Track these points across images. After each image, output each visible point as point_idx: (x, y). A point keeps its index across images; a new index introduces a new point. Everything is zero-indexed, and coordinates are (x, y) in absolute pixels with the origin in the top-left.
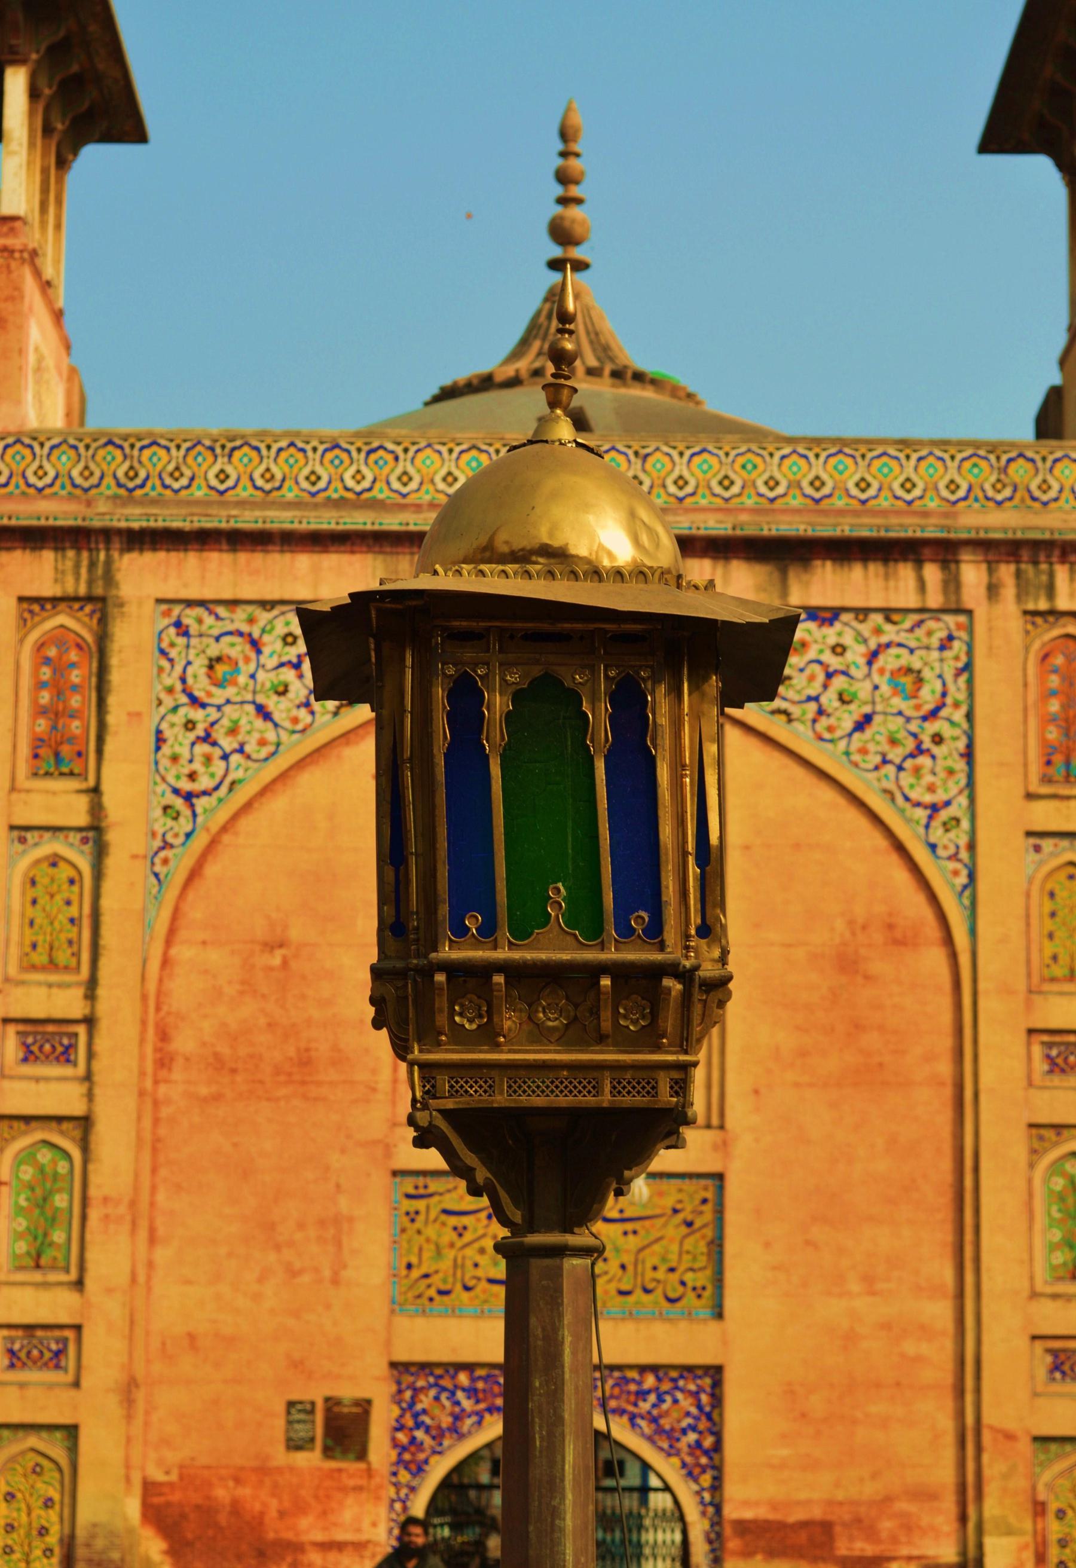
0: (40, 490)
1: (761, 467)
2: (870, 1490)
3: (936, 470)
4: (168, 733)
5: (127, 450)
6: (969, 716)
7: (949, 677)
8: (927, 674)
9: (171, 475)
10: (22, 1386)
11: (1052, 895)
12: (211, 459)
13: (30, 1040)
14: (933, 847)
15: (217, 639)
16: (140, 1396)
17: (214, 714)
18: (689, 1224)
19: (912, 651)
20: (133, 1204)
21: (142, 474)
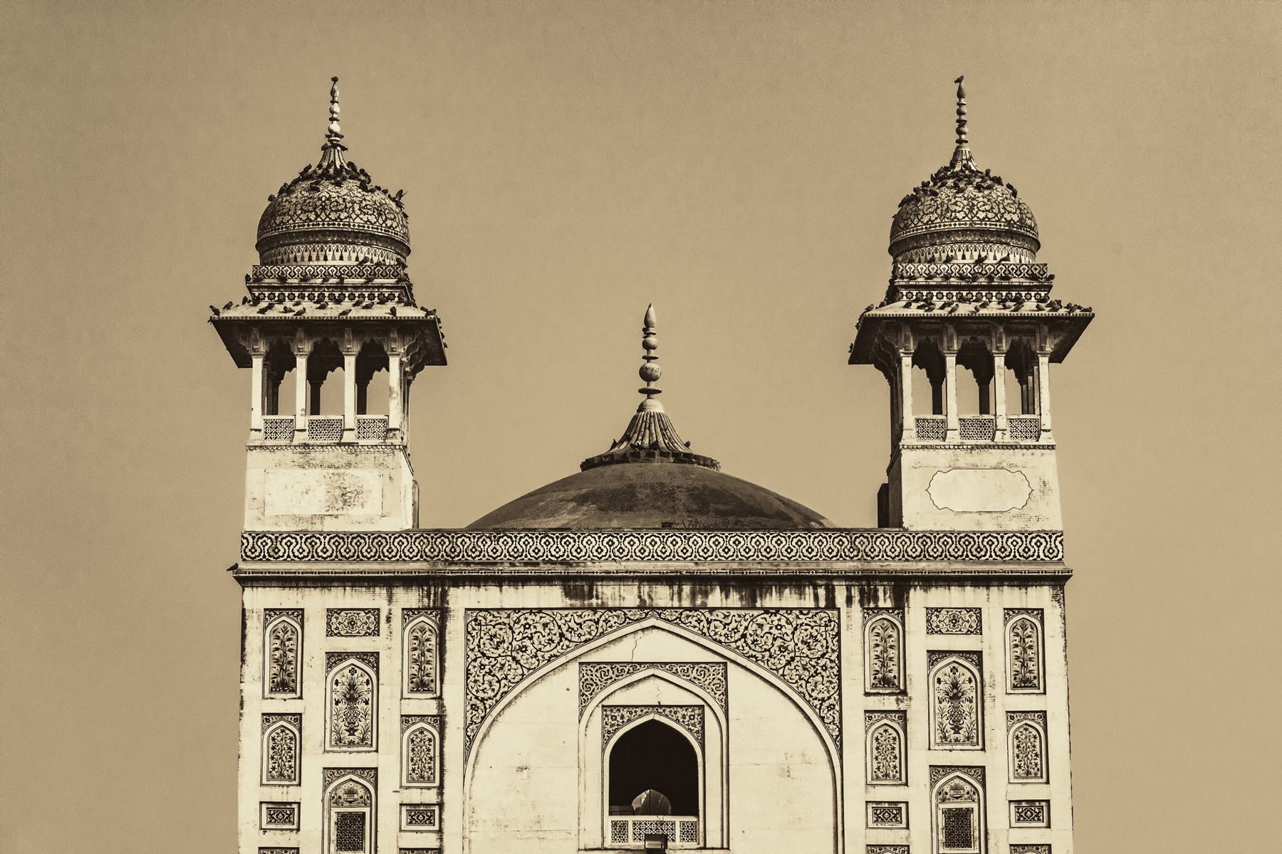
0: (411, 558)
1: (743, 543)
3: (823, 543)
4: (472, 671)
5: (451, 539)
6: (839, 657)
7: (829, 640)
8: (819, 637)
9: (471, 550)
11: (877, 739)
12: (489, 543)
13: (413, 813)
14: (822, 718)
15: (494, 627)
17: (494, 662)
19: (812, 628)
21: (458, 550)
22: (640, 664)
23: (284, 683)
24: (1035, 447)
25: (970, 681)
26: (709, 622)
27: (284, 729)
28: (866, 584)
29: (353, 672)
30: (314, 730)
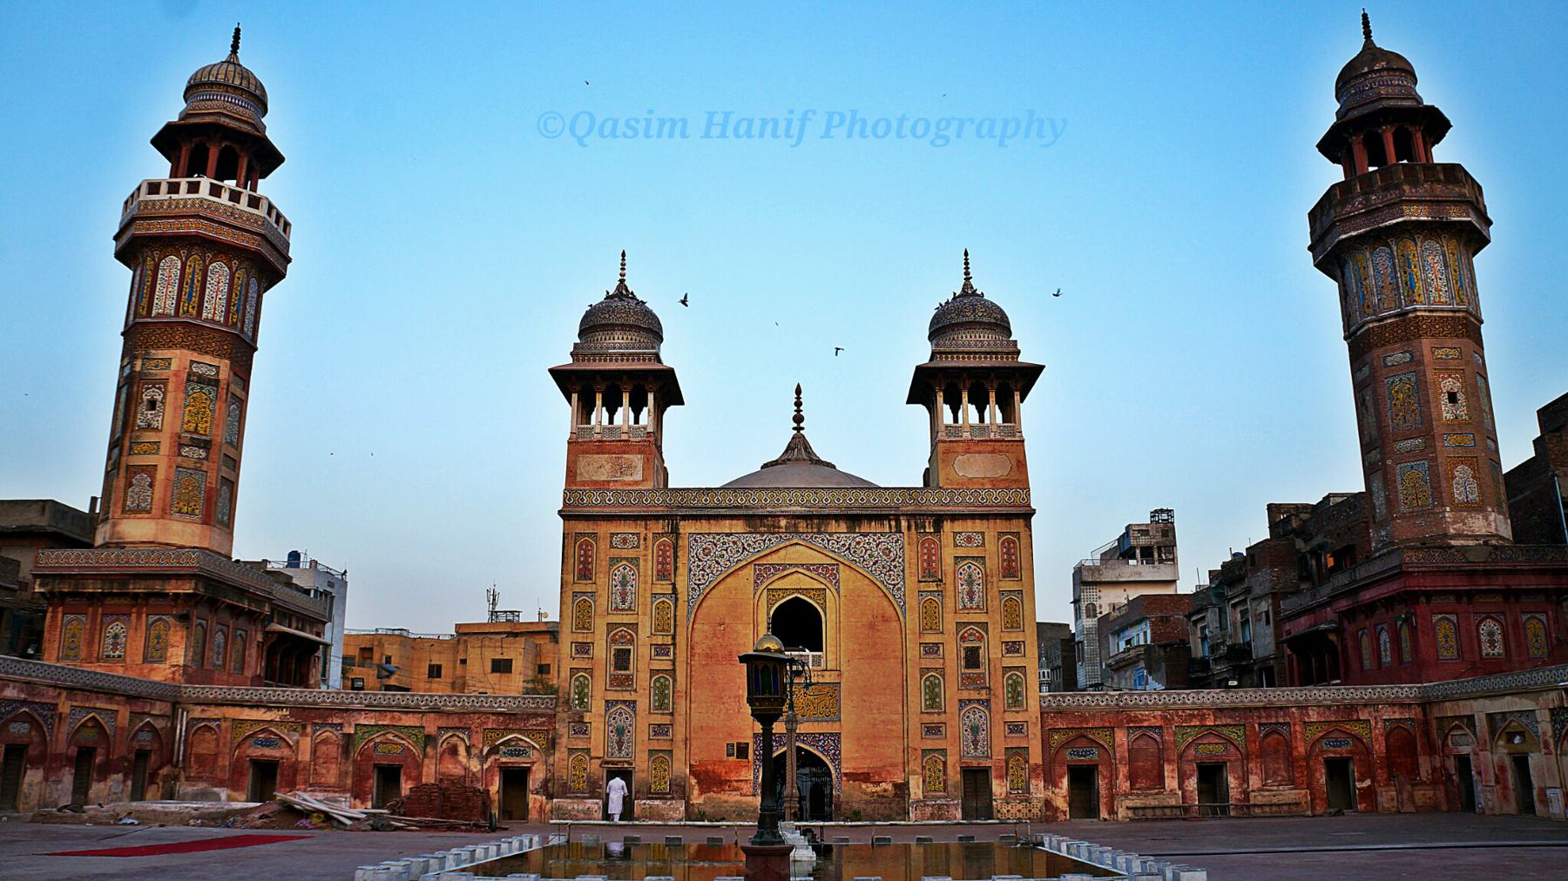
2: (879, 764)
10: (658, 740)
16: (688, 742)
18: (831, 696)
20: (686, 692)
22: (790, 565)
23: (585, 573)
24: (1014, 441)
25: (979, 574)
26: (829, 541)
27: (585, 601)
28: (916, 518)
29: (624, 569)
30: (603, 601)
